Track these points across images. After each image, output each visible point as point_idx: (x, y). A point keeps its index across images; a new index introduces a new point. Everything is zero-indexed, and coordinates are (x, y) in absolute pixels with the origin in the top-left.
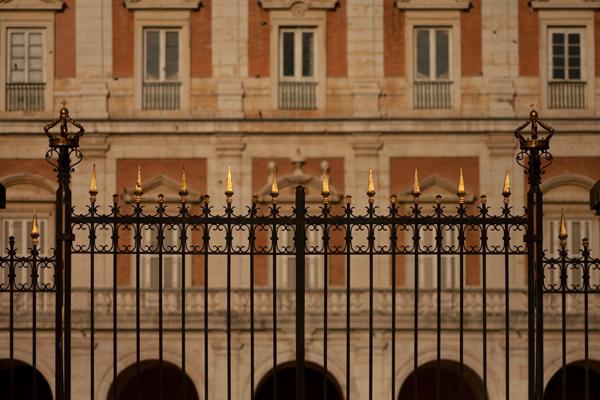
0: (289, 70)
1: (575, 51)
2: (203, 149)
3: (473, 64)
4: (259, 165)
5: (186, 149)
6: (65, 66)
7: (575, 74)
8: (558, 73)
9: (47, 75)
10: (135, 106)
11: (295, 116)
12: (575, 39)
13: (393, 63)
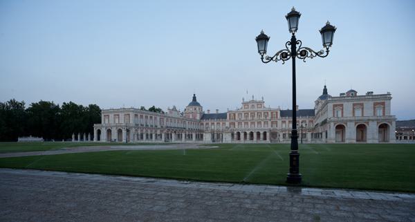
11: (253, 119)
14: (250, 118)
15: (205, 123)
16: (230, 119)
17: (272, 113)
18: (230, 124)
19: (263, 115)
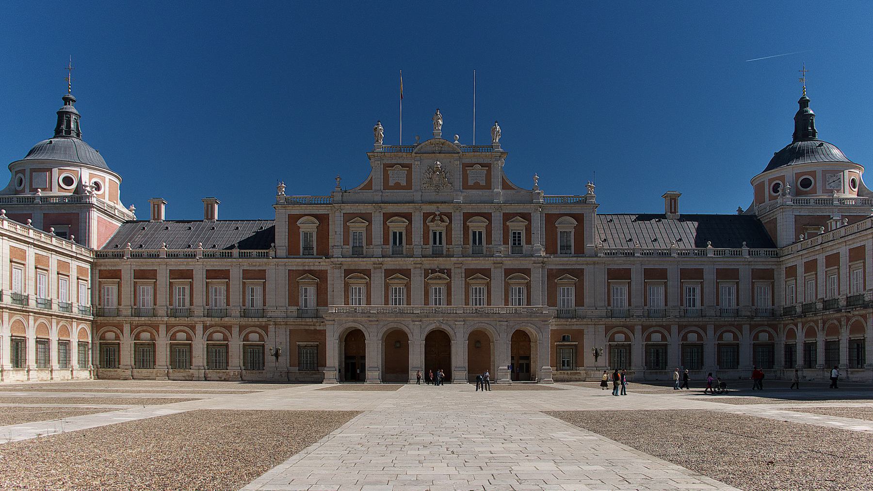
0: (435, 243)
1: (519, 237)
6: (369, 242)
7: (519, 244)
8: (515, 244)
9: (364, 244)
12: (519, 233)
13: (466, 242)
17: (550, 220)
19: (497, 234)
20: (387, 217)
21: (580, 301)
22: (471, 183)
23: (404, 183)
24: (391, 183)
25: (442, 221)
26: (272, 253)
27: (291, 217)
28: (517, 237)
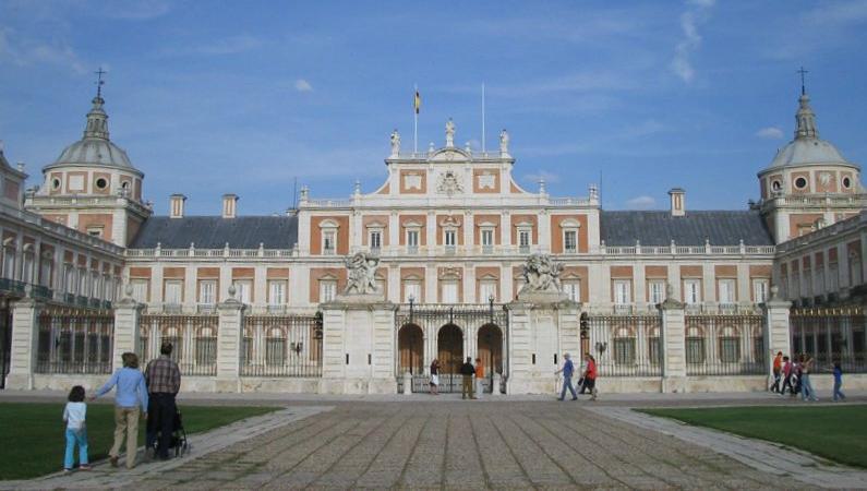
2: (424, 265)
3: (498, 241)
4: (440, 270)
5: (419, 265)
10: (406, 253)
14: (433, 247)
15: (157, 270)
16: (315, 248)
18: (317, 278)
19: (506, 235)
20: (403, 218)
21: (585, 296)
22: (481, 187)
23: (419, 187)
24: (407, 187)
25: (454, 221)
26: (295, 254)
27: (313, 218)
28: (524, 238)
